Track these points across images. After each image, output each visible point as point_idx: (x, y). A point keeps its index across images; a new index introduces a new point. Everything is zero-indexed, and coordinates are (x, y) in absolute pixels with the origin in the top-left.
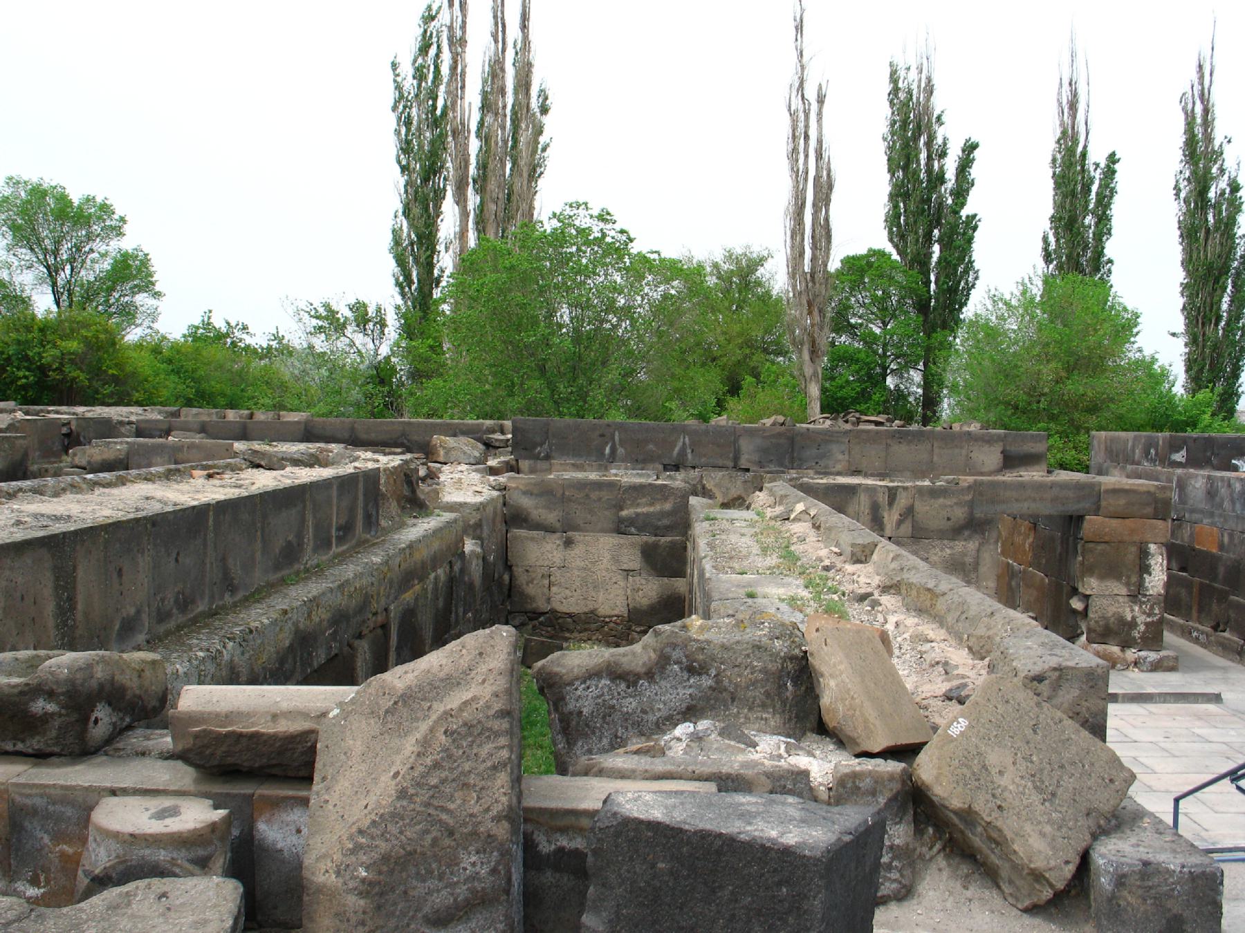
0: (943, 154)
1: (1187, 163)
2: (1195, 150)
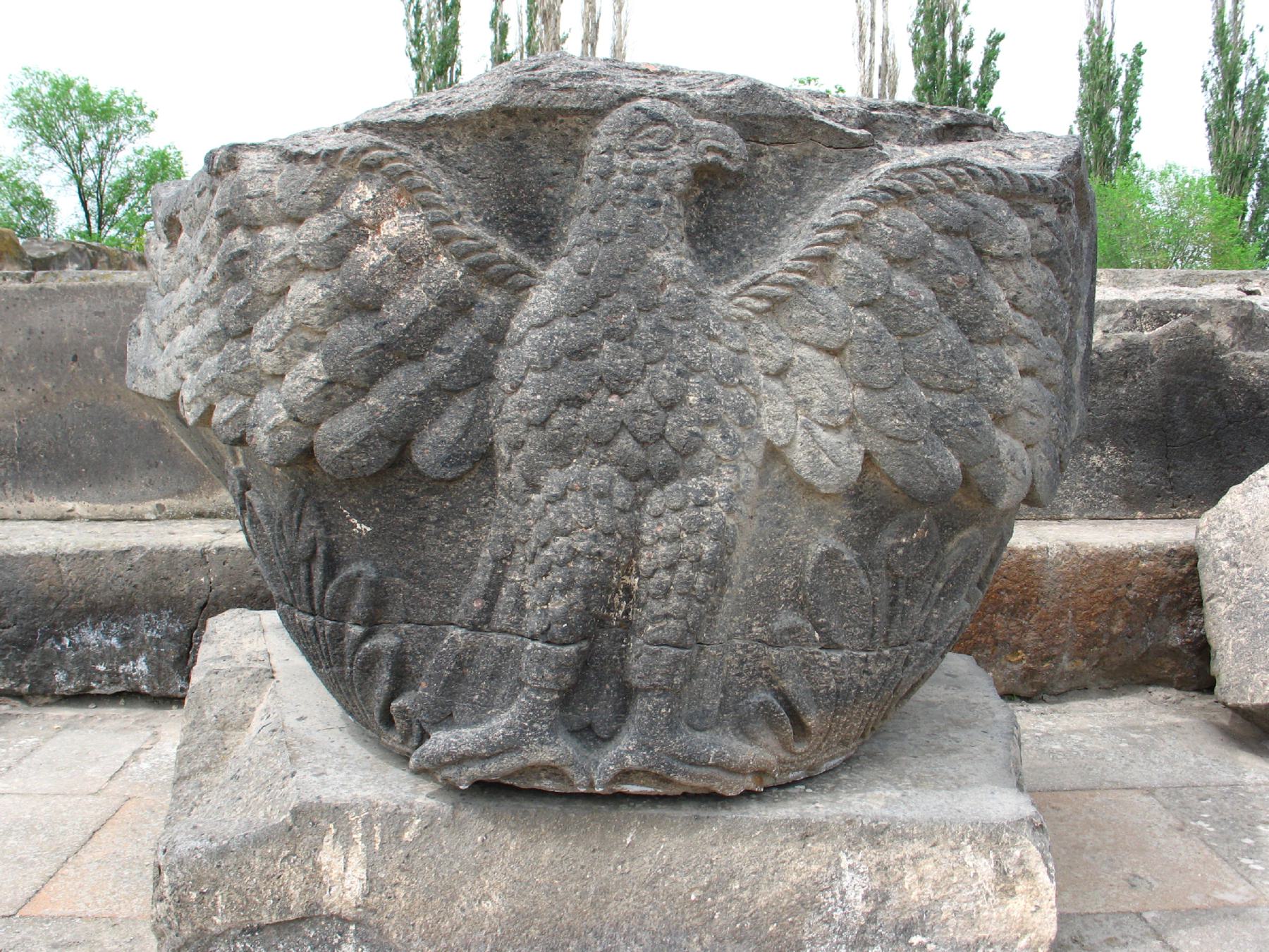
0: (968, 46)
1: (1216, 53)
2: (1226, 39)
